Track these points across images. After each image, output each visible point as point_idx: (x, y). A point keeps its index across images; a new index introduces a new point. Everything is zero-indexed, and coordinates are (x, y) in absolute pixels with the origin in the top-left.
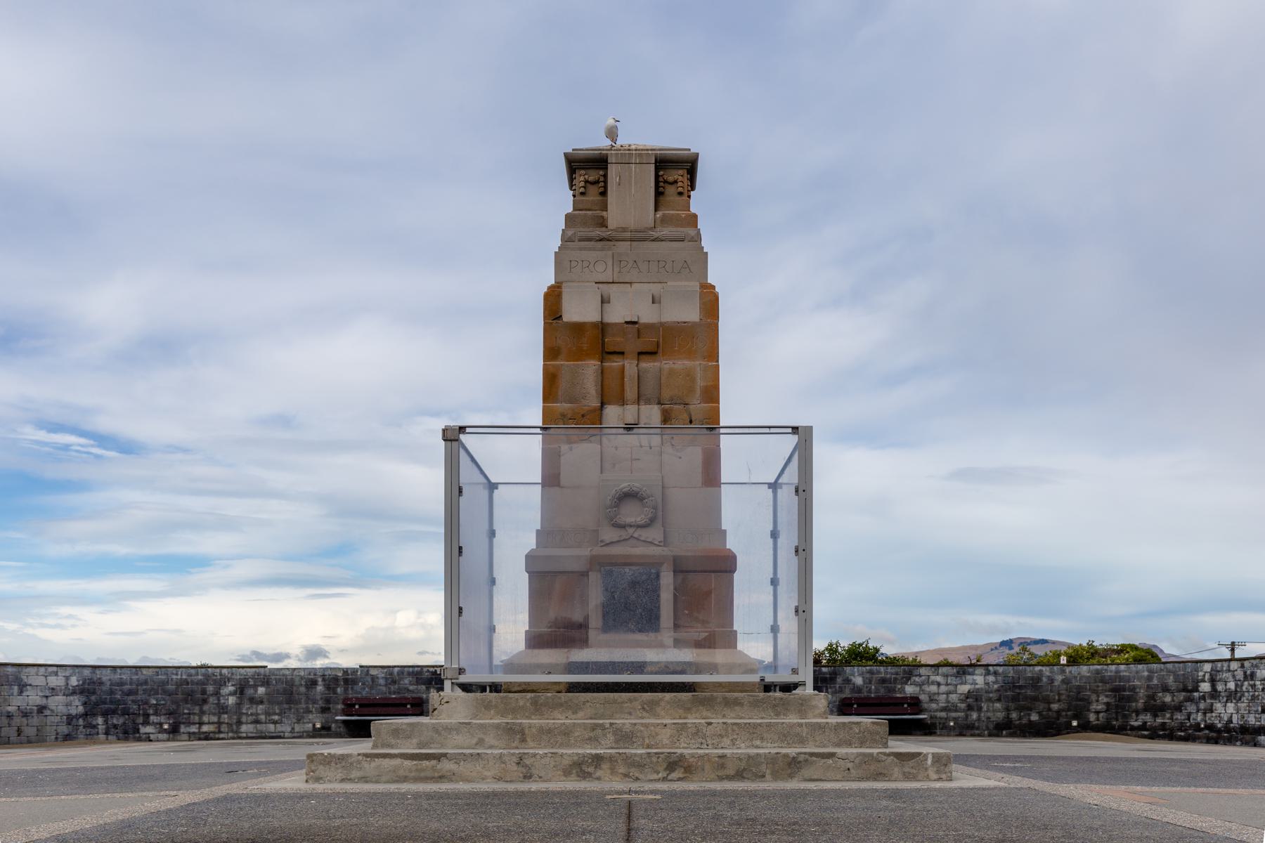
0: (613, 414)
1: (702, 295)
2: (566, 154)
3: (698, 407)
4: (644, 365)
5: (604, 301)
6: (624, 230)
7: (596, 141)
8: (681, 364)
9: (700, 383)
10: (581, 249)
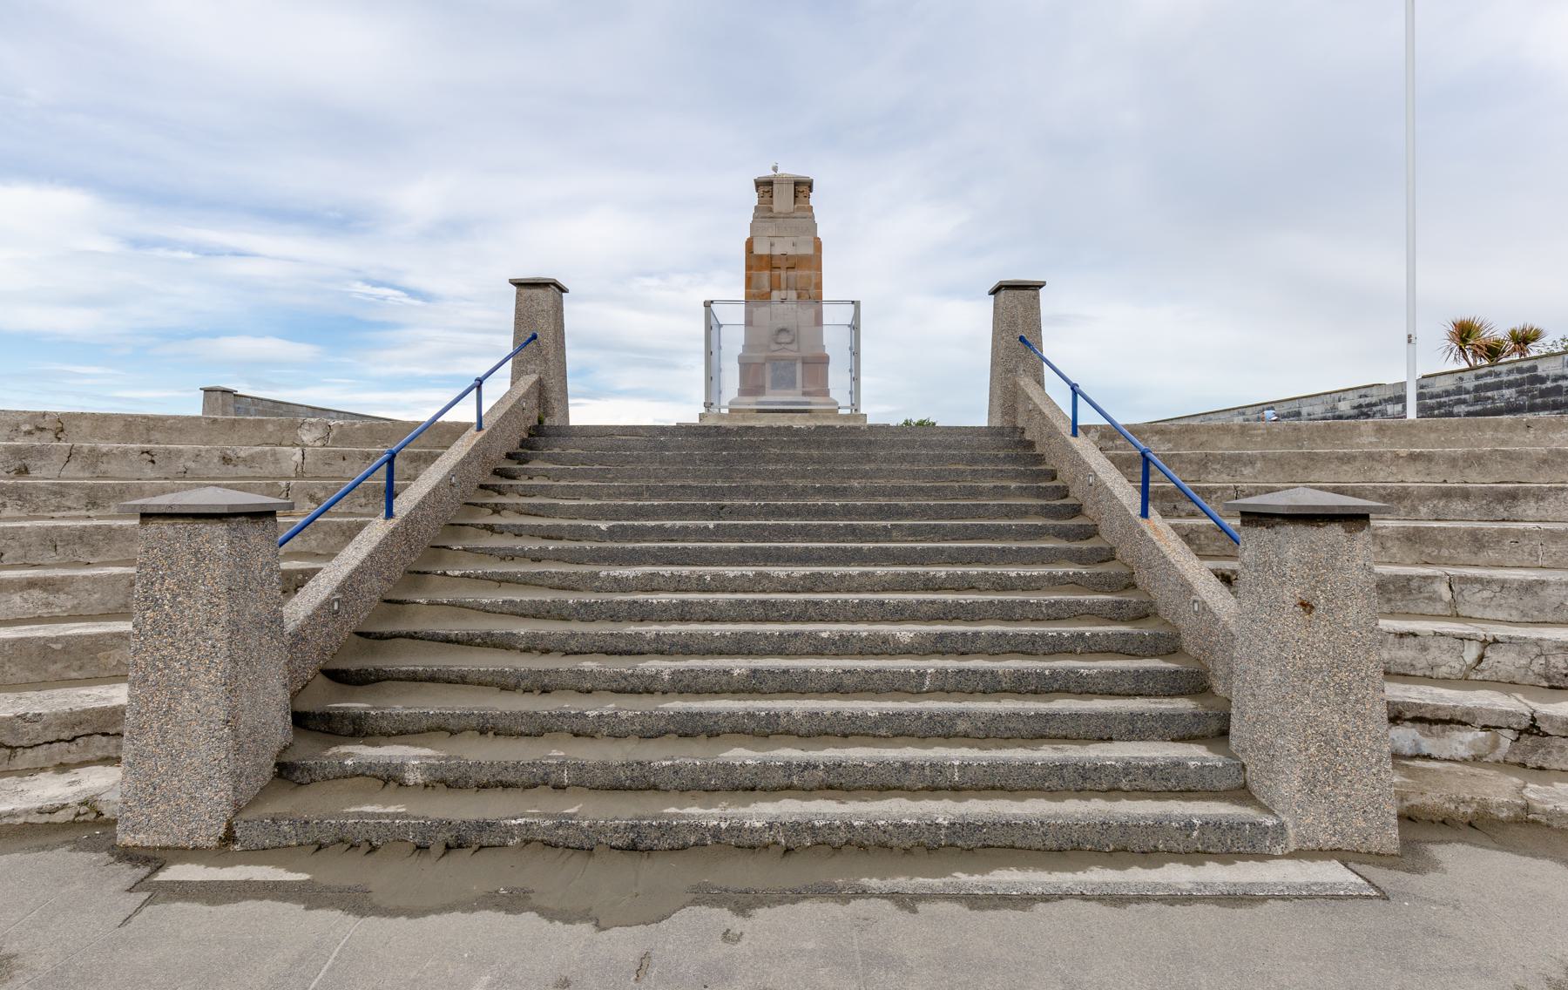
0: (776, 295)
1: (815, 243)
2: (755, 180)
3: (813, 292)
4: (788, 273)
5: (772, 245)
6: (780, 213)
7: (767, 173)
8: (806, 272)
9: (814, 281)
10: (761, 222)
